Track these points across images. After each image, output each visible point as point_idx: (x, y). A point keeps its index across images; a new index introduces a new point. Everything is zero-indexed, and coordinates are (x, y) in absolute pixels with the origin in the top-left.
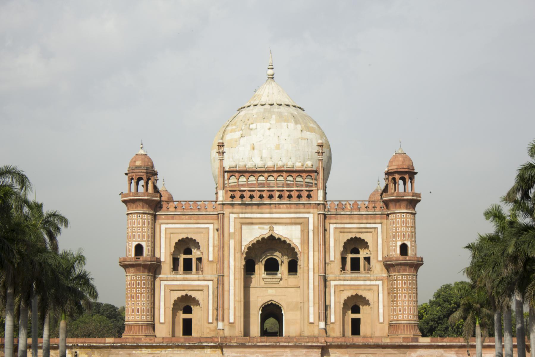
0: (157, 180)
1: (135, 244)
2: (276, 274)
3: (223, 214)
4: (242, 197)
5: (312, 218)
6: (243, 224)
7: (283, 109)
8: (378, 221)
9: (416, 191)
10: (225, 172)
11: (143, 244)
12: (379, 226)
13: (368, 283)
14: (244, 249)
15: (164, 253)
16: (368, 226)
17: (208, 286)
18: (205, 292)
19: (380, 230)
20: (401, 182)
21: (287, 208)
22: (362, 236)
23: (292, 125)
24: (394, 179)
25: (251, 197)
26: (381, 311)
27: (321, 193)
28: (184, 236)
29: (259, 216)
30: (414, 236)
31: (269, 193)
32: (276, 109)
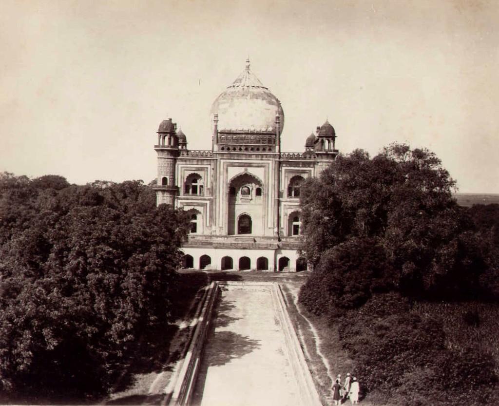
1: (162, 177)
2: (248, 197)
3: (217, 160)
5: (271, 163)
6: (228, 166)
8: (312, 166)
9: (336, 148)
10: (218, 133)
11: (168, 177)
14: (229, 181)
15: (180, 183)
17: (207, 204)
18: (205, 207)
20: (327, 142)
21: (256, 157)
27: (277, 147)
28: (193, 172)
31: (245, 148)
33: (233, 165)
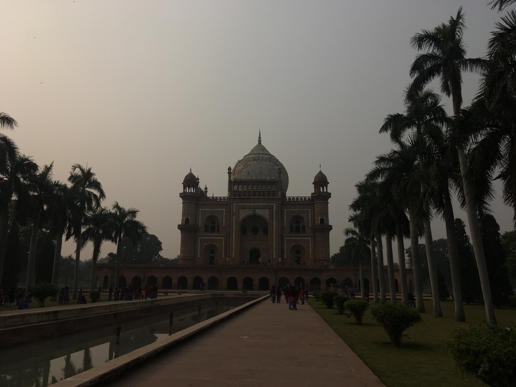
0: (206, 192)
4: (239, 195)
7: (264, 156)
11: (190, 218)
12: (310, 210)
13: (304, 238)
15: (201, 223)
16: (304, 209)
19: (310, 212)
22: (301, 215)
23: (268, 163)
24: (317, 186)
25: (244, 195)
26: (311, 253)
27: (280, 193)
29: (248, 204)
30: (327, 215)
32: (261, 156)
33: (244, 208)
